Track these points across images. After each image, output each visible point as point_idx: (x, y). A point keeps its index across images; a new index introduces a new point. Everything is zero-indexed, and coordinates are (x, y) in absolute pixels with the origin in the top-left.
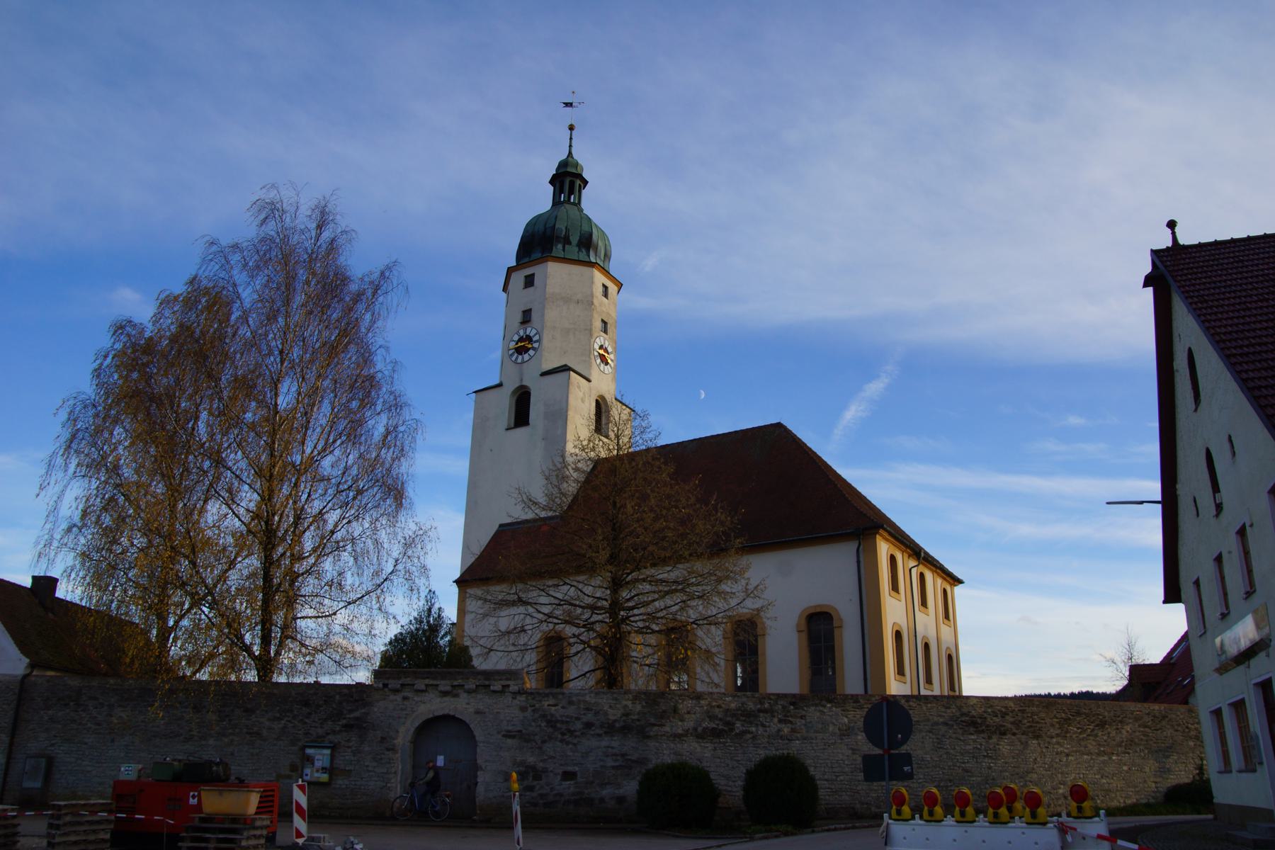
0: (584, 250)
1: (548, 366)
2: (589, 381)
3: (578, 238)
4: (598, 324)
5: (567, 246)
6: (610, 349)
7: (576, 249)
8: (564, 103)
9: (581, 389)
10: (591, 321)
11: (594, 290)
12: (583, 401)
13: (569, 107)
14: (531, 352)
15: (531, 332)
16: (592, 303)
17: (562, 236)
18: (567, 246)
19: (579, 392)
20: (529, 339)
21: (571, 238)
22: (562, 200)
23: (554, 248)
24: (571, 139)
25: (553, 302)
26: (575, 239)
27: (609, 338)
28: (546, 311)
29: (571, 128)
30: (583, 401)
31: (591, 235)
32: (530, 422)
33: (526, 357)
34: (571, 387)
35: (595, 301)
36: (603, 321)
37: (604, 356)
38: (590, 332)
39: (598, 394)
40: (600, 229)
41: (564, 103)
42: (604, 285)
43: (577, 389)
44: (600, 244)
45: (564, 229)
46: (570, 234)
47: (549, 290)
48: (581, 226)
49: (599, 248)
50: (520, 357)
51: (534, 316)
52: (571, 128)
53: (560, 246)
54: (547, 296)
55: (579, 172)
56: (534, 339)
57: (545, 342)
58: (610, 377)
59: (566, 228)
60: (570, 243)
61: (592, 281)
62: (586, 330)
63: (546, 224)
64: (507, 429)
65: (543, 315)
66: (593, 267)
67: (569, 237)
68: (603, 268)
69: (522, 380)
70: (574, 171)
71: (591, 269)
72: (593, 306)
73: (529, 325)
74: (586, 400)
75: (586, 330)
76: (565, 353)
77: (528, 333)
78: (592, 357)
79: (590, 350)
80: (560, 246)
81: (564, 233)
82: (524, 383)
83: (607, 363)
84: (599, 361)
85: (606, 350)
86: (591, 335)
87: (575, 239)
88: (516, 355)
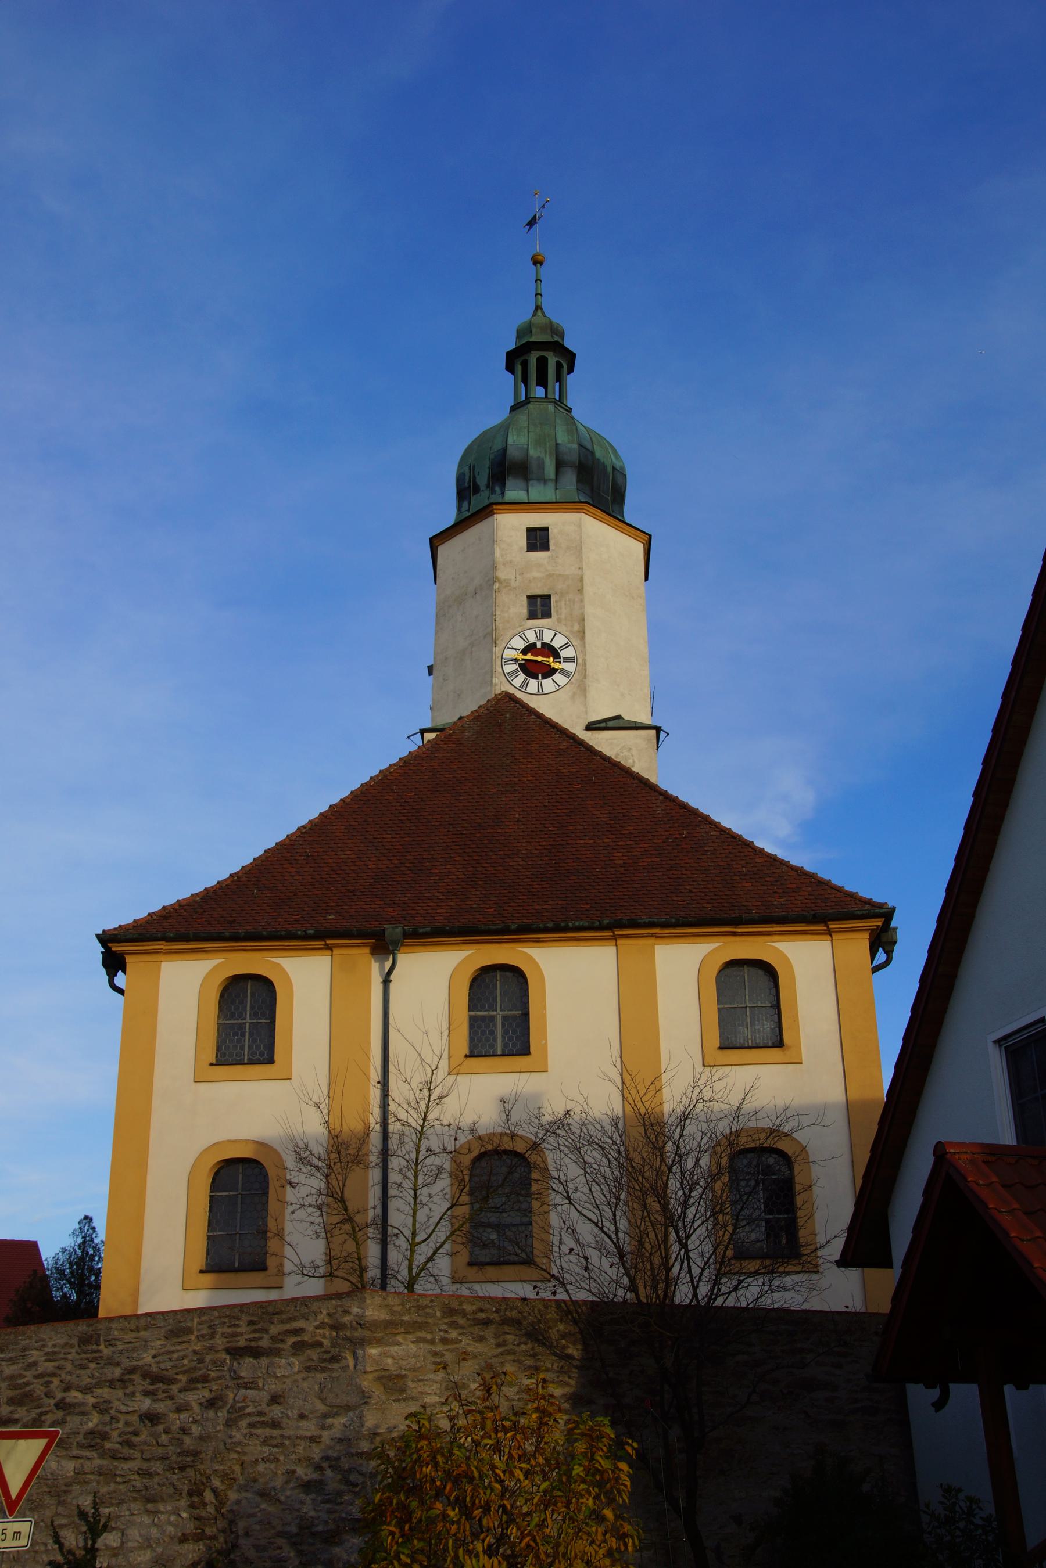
3: (487, 471)
6: (557, 644)
10: (493, 615)
11: (498, 553)
16: (495, 580)
17: (466, 485)
26: (482, 481)
27: (559, 620)
35: (502, 574)
36: (532, 598)
37: (536, 661)
38: (491, 637)
42: (531, 531)
66: (491, 514)
71: (489, 519)
72: (496, 586)
75: (485, 637)
76: (459, 695)
81: (467, 478)
87: (482, 481)
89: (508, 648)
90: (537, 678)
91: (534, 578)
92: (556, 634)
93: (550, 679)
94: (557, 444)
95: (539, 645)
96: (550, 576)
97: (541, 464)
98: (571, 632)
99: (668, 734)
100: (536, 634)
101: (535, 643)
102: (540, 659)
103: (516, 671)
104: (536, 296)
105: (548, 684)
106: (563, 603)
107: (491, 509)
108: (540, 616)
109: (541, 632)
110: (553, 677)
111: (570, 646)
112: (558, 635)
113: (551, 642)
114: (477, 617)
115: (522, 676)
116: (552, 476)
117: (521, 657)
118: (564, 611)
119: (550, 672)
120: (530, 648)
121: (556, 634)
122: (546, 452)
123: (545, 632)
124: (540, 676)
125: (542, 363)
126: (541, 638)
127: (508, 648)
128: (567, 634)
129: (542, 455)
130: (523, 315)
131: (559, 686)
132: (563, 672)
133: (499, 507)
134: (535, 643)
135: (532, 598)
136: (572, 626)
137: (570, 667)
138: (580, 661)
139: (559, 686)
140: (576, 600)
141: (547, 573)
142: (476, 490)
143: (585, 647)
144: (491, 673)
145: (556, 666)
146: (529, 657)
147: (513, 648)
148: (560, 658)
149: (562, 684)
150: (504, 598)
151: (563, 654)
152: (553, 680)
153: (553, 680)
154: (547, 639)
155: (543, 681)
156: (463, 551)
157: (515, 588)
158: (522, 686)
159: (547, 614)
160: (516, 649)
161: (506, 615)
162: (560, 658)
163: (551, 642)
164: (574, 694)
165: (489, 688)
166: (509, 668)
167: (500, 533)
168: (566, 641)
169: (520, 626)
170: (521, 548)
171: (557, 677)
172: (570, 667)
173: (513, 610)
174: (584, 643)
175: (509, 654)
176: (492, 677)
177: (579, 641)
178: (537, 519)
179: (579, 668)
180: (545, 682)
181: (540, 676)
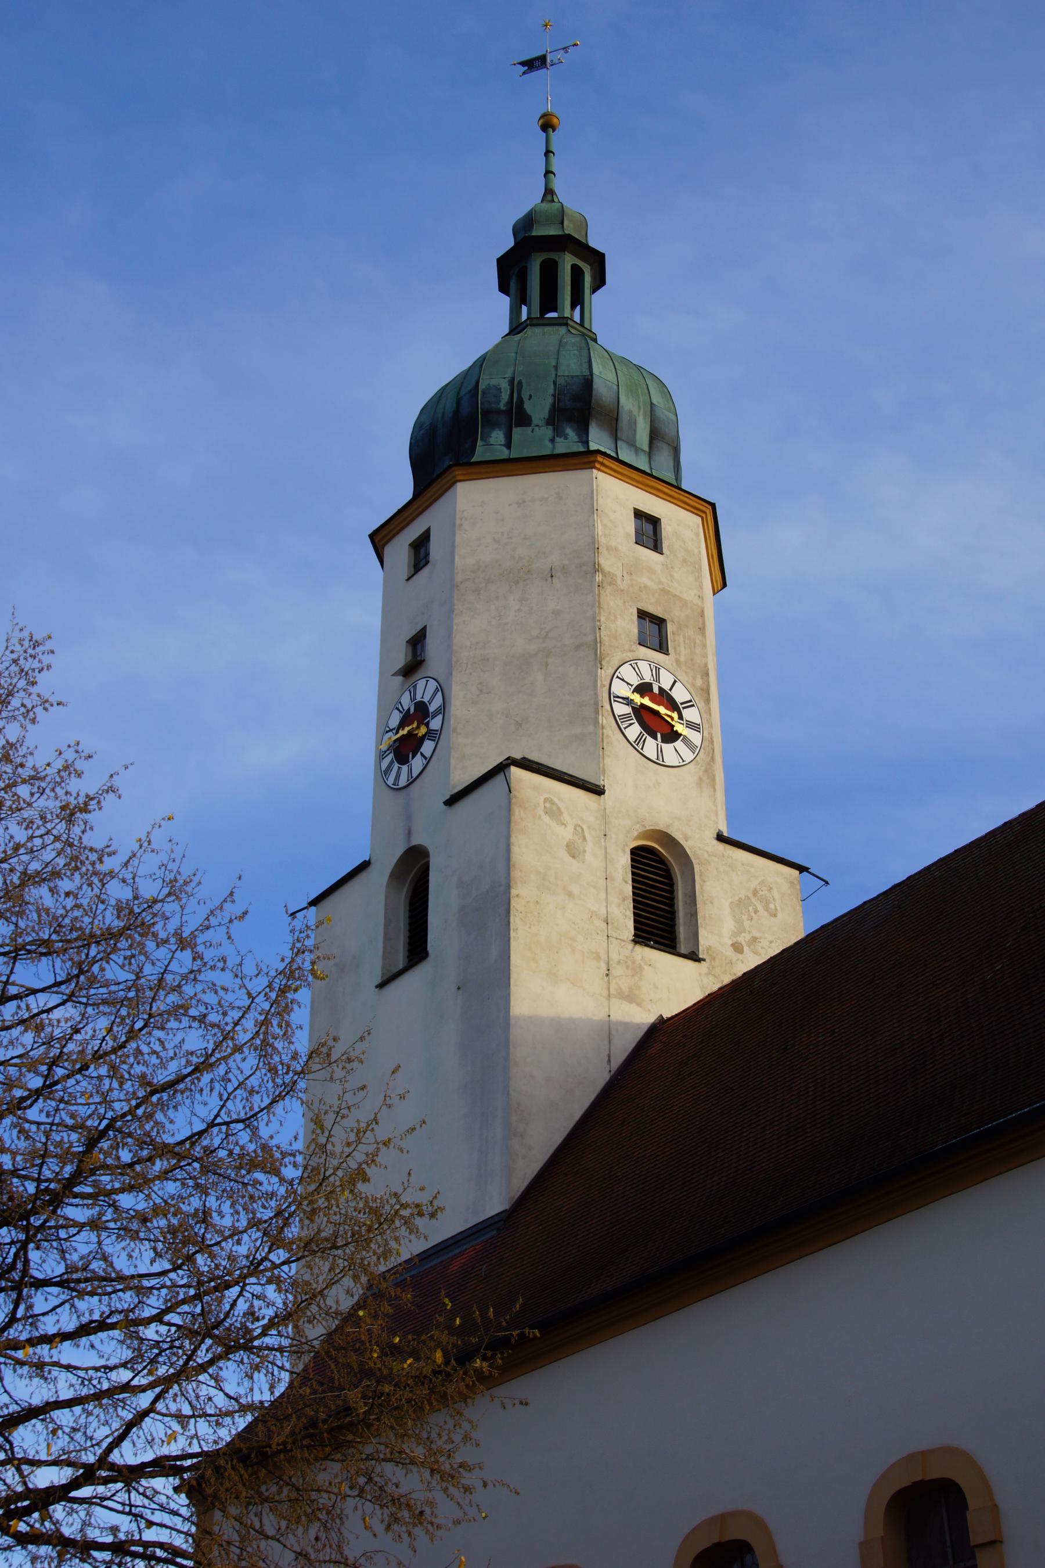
0: (569, 431)
1: (461, 778)
2: (598, 791)
3: (550, 400)
4: (628, 625)
5: (517, 432)
6: (680, 695)
7: (548, 432)
8: (523, 64)
9: (566, 816)
10: (595, 619)
11: (600, 530)
12: (573, 851)
13: (538, 68)
14: (427, 747)
15: (425, 690)
16: (596, 568)
17: (502, 406)
18: (517, 432)
19: (559, 830)
20: (421, 712)
21: (528, 406)
22: (524, 317)
23: (479, 443)
24: (548, 152)
25: (477, 591)
26: (539, 408)
27: (677, 661)
28: (457, 620)
29: (547, 125)
30: (573, 851)
31: (588, 382)
32: (430, 948)
33: (417, 763)
34: (517, 813)
35: (607, 561)
36: (642, 614)
37: (657, 713)
39: (639, 829)
40: (625, 361)
41: (523, 64)
42: (639, 514)
43: (546, 819)
44: (627, 404)
45: (505, 385)
46: (525, 396)
47: (464, 559)
48: (556, 368)
49: (624, 418)
50: (405, 768)
51: (432, 646)
52: (547, 125)
53: (497, 436)
54: (458, 578)
55: (569, 228)
56: (432, 708)
57: (458, 708)
58: (689, 775)
59: (512, 382)
60: (524, 420)
61: (590, 506)
62: (578, 648)
63: (458, 393)
64: (381, 986)
65: (449, 636)
66: (590, 465)
67: (521, 401)
68: (651, 475)
69: (409, 833)
70: (553, 231)
72: (599, 577)
73: (421, 673)
74: (589, 847)
75: (578, 648)
76: (519, 725)
77: (418, 699)
78: (606, 720)
79: (596, 704)
80: (497, 436)
81: (505, 397)
82: (416, 841)
83: (672, 736)
84: (634, 730)
85: (665, 698)
86: (598, 661)
87: (539, 408)
88: (396, 765)
90: (656, 738)
91: (646, 587)
92: (675, 682)
94: (652, 404)
95: (656, 690)
96: (665, 592)
97: (633, 424)
98: (693, 685)
99: (827, 883)
102: (662, 710)
104: (545, 176)
106: (681, 639)
107: (592, 459)
109: (658, 670)
111: (693, 706)
114: (556, 613)
116: (646, 448)
117: (637, 699)
118: (684, 652)
119: (672, 736)
120: (643, 689)
121: (675, 682)
122: (639, 407)
124: (659, 735)
125: (577, 273)
126: (658, 680)
128: (689, 687)
129: (635, 410)
130: (530, 199)
132: (687, 741)
133: (607, 462)
134: (651, 684)
135: (642, 614)
136: (694, 678)
137: (695, 737)
138: (706, 734)
140: (697, 641)
141: (661, 586)
142: (524, 420)
143: (710, 714)
144: (597, 709)
145: (679, 728)
146: (646, 701)
149: (688, 759)
150: (610, 600)
151: (687, 714)
154: (666, 686)
155: (664, 746)
156: (519, 504)
157: (622, 591)
161: (612, 626)
164: (700, 779)
165: (591, 729)
166: (621, 709)
167: (600, 501)
168: (689, 698)
169: (631, 651)
170: (628, 535)
171: (679, 744)
172: (695, 737)
173: (619, 622)
174: (710, 709)
175: (621, 689)
176: (597, 713)
177: (703, 704)
179: (705, 744)
181: (659, 735)
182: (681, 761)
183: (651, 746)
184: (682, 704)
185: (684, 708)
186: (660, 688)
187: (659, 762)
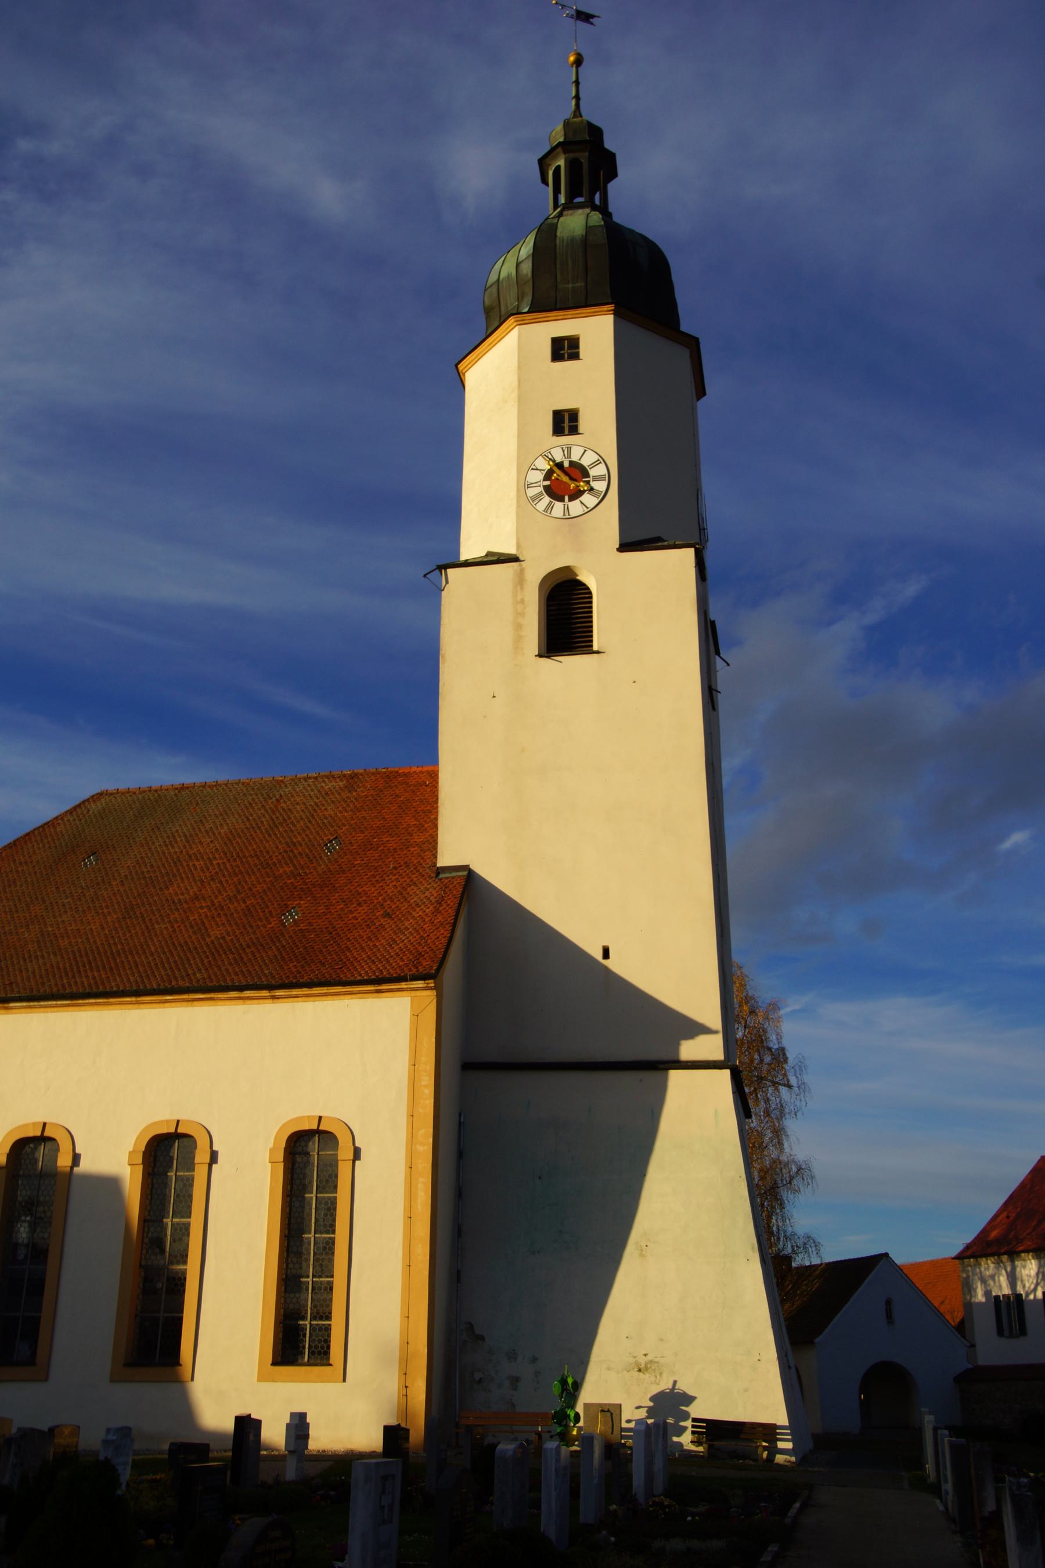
89: (532, 469)
92: (585, 451)
93: (577, 502)
100: (563, 451)
101: (562, 462)
103: (541, 494)
105: (575, 507)
108: (567, 432)
109: (569, 449)
110: (582, 498)
111: (600, 463)
112: (589, 452)
113: (580, 460)
115: (547, 499)
121: (585, 451)
123: (574, 450)
124: (566, 498)
126: (569, 456)
127: (532, 469)
131: (587, 508)
134: (562, 462)
139: (587, 508)
147: (537, 469)
148: (589, 477)
151: (593, 472)
152: (581, 503)
153: (581, 503)
154: (575, 458)
158: (546, 510)
159: (574, 430)
160: (541, 470)
162: (589, 477)
163: (580, 460)
168: (596, 457)
178: (564, 327)
180: (571, 504)
181: (566, 498)
182: (585, 508)
183: (558, 506)
184: (589, 466)
185: (590, 468)
186: (571, 463)
187: (567, 517)
